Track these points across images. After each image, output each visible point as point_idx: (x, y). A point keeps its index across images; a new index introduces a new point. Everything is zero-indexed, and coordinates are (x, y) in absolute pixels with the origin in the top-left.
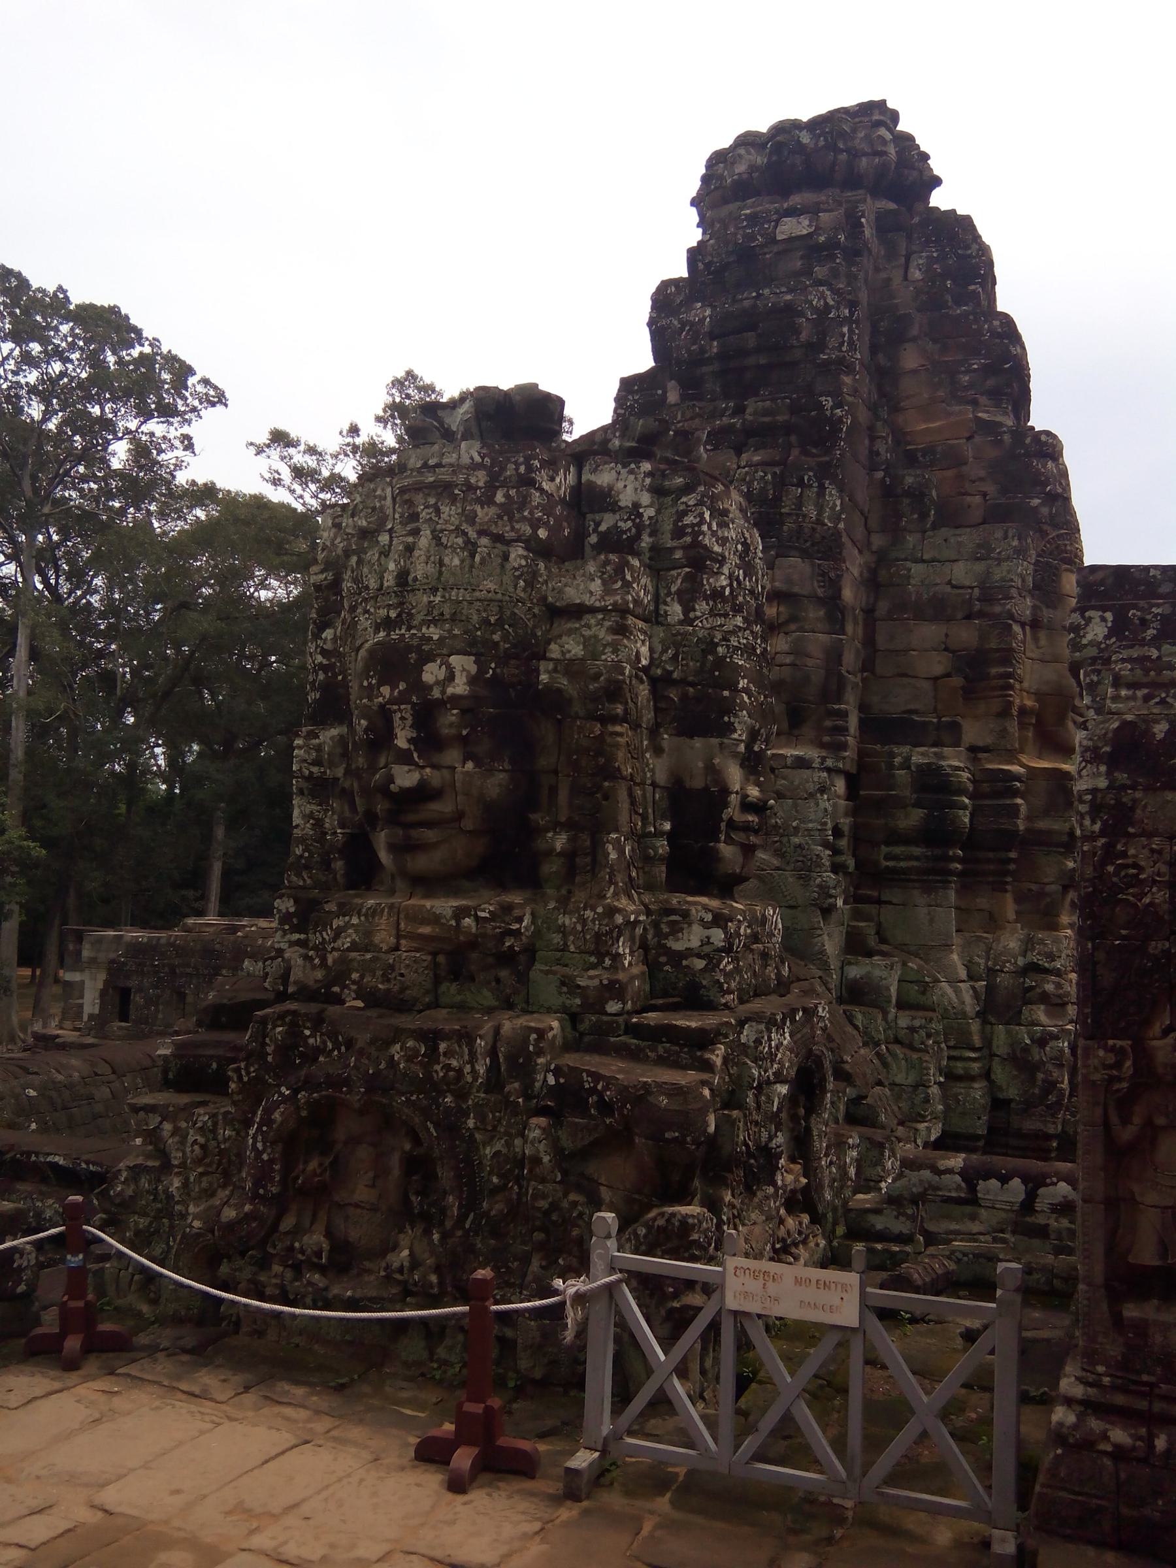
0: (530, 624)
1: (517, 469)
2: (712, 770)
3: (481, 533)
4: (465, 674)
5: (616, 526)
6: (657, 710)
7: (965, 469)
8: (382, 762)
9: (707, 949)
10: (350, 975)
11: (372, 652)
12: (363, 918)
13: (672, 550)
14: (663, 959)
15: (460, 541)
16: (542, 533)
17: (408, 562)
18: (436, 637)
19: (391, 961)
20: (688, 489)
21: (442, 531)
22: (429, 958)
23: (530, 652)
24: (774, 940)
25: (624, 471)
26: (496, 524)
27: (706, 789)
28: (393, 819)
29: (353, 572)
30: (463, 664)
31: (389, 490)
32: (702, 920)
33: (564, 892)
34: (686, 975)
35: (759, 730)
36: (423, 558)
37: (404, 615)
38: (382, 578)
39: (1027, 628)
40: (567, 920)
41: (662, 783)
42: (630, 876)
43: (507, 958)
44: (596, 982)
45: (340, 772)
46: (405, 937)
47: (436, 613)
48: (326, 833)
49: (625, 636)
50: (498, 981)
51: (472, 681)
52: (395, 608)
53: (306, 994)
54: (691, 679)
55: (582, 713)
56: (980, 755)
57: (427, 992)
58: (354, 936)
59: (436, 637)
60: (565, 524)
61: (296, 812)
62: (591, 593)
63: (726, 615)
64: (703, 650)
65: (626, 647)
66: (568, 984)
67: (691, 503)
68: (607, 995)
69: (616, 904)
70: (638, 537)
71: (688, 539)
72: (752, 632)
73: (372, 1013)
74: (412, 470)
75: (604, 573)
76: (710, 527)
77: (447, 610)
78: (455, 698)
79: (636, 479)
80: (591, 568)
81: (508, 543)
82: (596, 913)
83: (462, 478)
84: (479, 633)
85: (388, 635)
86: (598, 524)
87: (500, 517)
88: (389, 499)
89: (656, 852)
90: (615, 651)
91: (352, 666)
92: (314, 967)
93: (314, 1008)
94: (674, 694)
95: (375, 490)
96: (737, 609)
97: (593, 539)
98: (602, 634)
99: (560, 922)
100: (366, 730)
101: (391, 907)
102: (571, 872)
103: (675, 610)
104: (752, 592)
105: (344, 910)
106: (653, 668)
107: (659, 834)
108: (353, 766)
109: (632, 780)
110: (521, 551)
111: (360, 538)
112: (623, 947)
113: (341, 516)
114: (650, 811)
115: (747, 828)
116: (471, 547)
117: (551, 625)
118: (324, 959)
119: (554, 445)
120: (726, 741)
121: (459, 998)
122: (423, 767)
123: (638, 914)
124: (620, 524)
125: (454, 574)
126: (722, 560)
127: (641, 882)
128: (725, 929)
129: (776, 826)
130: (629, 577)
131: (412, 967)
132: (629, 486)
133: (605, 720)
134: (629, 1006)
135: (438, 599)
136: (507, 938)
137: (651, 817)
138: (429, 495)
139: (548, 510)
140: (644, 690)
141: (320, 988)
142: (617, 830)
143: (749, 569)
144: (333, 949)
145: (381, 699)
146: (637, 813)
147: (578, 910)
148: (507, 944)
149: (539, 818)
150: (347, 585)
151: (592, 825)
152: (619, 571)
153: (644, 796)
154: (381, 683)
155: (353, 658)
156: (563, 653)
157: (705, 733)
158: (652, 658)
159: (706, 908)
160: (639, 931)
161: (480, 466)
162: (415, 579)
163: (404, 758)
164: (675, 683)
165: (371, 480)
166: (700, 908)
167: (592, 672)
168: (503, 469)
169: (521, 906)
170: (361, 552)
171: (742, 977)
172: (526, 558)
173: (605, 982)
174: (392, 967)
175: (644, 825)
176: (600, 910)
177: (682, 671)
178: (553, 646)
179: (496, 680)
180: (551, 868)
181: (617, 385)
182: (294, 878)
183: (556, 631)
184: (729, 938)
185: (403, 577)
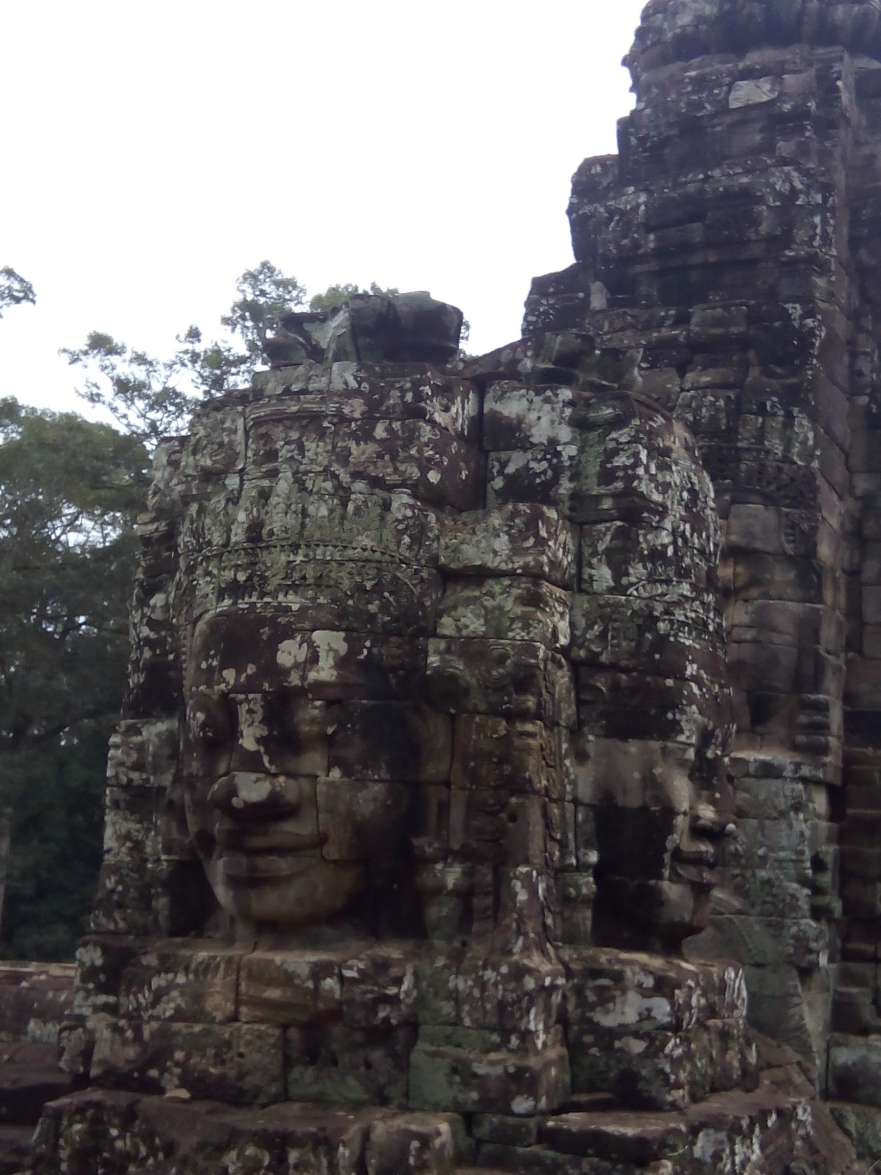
0: (417, 591)
1: (402, 397)
2: (651, 783)
3: (356, 475)
4: (331, 654)
5: (527, 468)
6: (579, 702)
8: (222, 767)
9: (647, 1026)
10: (172, 1053)
11: (213, 625)
12: (191, 976)
13: (599, 498)
14: (588, 1039)
15: (329, 485)
16: (433, 477)
17: (263, 512)
18: (295, 607)
19: (227, 1036)
20: (619, 422)
21: (306, 473)
22: (277, 1032)
23: (416, 626)
24: (736, 1013)
25: (537, 400)
26: (375, 464)
28: (235, 844)
29: (192, 523)
30: (330, 642)
31: (240, 422)
32: (640, 985)
33: (457, 944)
34: (619, 1061)
35: (713, 730)
36: (282, 506)
37: (256, 579)
38: (229, 531)
40: (461, 983)
41: (587, 800)
42: (544, 925)
43: (381, 1035)
44: (499, 1070)
45: (167, 779)
46: (246, 1003)
47: (296, 575)
48: (146, 860)
50: (368, 1065)
51: (341, 663)
52: (245, 570)
53: (115, 1079)
54: (624, 663)
55: (482, 707)
57: (274, 1079)
58: (179, 1001)
59: (295, 607)
60: (462, 464)
61: (109, 832)
62: (495, 553)
63: (668, 582)
64: (639, 626)
65: (540, 621)
66: (460, 1070)
67: (623, 440)
68: (513, 1088)
69: (526, 961)
70: (555, 481)
71: (620, 485)
72: (703, 603)
73: (201, 1107)
74: (270, 397)
75: (511, 527)
76: (647, 470)
77: (311, 572)
78: (319, 686)
79: (553, 409)
80: (496, 520)
81: (391, 488)
82: (499, 973)
83: (332, 407)
84: (350, 602)
85: (235, 603)
86: (504, 465)
87: (380, 456)
88: (241, 432)
89: (578, 890)
90: (526, 627)
91: (187, 642)
92: (125, 1042)
93: (123, 1098)
94: (601, 683)
95: (223, 422)
96: (683, 574)
97: (498, 483)
98: (509, 605)
99: (451, 985)
100: (203, 726)
101: (229, 961)
102: (466, 917)
103: (603, 575)
104: (702, 552)
105: (167, 965)
106: (575, 649)
107: (582, 867)
108: (185, 773)
109: (547, 795)
110: (406, 499)
111: (201, 481)
112: (535, 1022)
113: (180, 452)
114: (571, 836)
115: (698, 861)
116: (343, 493)
117: (444, 591)
118: (138, 1031)
119: (449, 366)
120: (670, 744)
121: (315, 1089)
122: (275, 775)
123: (554, 975)
124: (533, 465)
125: (320, 527)
126: (662, 511)
127: (559, 932)
128: (671, 998)
129: (736, 855)
130: (543, 533)
131: (255, 1046)
132: (545, 418)
134: (543, 1103)
135: (299, 558)
136: (381, 1006)
137: (572, 846)
138: (291, 428)
139: (440, 446)
140: (562, 678)
141: (132, 1071)
142: (527, 862)
143: (697, 521)
144: (151, 1018)
145: (223, 686)
146: (553, 839)
147: (475, 969)
148: (381, 1015)
149: (425, 844)
150: (184, 539)
151: (495, 854)
152: (531, 525)
153: (563, 816)
154: (223, 666)
155: (189, 633)
156: (459, 630)
158: (573, 636)
159: (646, 970)
160: (556, 999)
161: (357, 393)
162: (271, 533)
163: (252, 763)
164: (603, 668)
165: (217, 409)
166: (637, 969)
167: (496, 653)
168: (385, 397)
169: (401, 963)
170: (203, 498)
171: (694, 1065)
172: (412, 507)
173: (511, 1070)
174: (228, 1044)
175: (563, 856)
176: (504, 970)
177: (612, 653)
178: (446, 620)
180: (439, 911)
181: (528, 287)
182: (103, 920)
183: (449, 601)
184: (677, 1011)
185: (255, 530)
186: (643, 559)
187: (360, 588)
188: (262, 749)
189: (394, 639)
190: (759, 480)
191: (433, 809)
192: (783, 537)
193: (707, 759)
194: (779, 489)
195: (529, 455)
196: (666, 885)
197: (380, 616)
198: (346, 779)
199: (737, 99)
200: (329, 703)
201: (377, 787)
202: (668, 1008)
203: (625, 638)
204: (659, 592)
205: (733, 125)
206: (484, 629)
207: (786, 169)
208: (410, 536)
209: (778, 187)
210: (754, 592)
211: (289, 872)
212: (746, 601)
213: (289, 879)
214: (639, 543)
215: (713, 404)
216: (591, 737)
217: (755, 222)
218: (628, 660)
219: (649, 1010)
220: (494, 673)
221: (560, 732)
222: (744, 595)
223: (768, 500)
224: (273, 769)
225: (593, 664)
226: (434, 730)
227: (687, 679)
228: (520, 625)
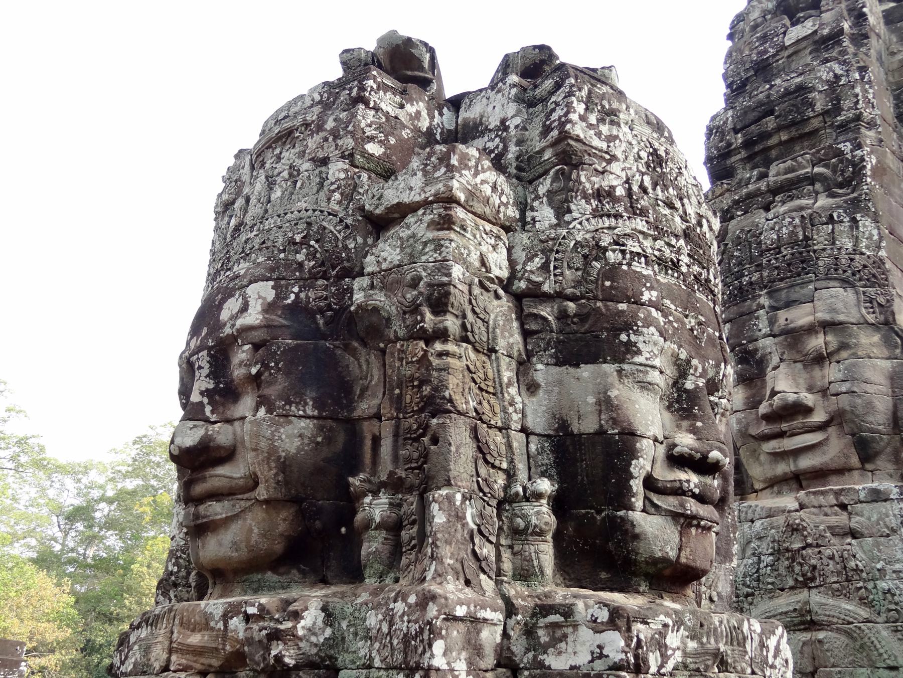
2: (605, 403)
6: (526, 334)
27: (601, 432)
41: (539, 430)
49: (450, 229)
54: (569, 291)
55: (401, 333)
62: (411, 189)
64: (585, 257)
65: (452, 241)
94: (546, 311)
103: (545, 215)
133: (430, 338)
151: (420, 479)
153: (509, 446)
157: (593, 359)
164: (546, 298)
178: (370, 259)
179: (297, 309)
186: (586, 197)
187: (292, 242)
188: (206, 400)
189: (321, 282)
190: (836, 270)
191: (368, 443)
192: (864, 311)
193: (687, 391)
194: (854, 274)
195: (486, 139)
196: (637, 516)
197: (306, 262)
198: (268, 415)
199: (790, 39)
200: (256, 347)
201: (303, 423)
202: (622, 643)
203: (569, 267)
204: (607, 225)
205: (789, 57)
206: (399, 257)
207: (828, 65)
208: (342, 194)
209: (824, 78)
210: (844, 354)
211: (224, 516)
212: (838, 362)
213: (227, 521)
214: (580, 183)
215: (790, 223)
216: (540, 366)
217: (812, 105)
218: (574, 287)
219: (600, 647)
220: (408, 296)
221: (497, 358)
222: (836, 357)
223: (846, 283)
224: (213, 418)
225: (535, 294)
226: (365, 367)
227: (643, 304)
228: (433, 246)
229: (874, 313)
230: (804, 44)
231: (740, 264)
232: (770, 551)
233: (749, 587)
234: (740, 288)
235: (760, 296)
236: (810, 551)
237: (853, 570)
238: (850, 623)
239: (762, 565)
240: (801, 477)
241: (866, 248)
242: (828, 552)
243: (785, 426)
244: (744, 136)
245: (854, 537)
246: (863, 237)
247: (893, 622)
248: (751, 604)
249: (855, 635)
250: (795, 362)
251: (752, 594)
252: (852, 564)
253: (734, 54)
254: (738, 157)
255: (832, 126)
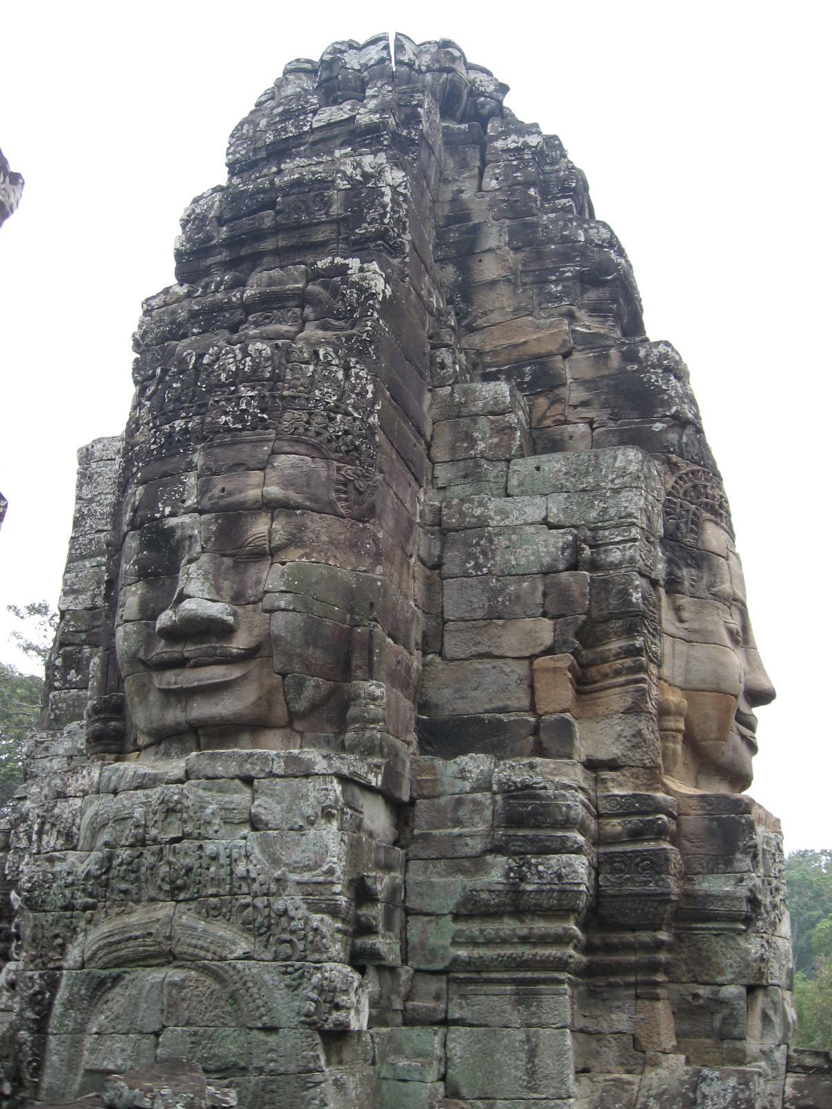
7: (563, 392)
39: (662, 590)
56: (607, 775)
212: (283, 564)
217: (327, 204)
229: (346, 500)
230: (336, 131)
231: (178, 399)
232: (131, 840)
233: (90, 895)
234: (169, 436)
235: (195, 451)
236: (186, 843)
237: (243, 878)
238: (223, 959)
239: (115, 863)
240: (200, 732)
241: (354, 407)
242: (210, 848)
243: (189, 650)
244: (231, 230)
245: (255, 829)
246: (352, 392)
247: (284, 960)
248: (89, 922)
249: (226, 976)
250: (223, 555)
251: (93, 907)
252: (241, 869)
253: (246, 127)
254: (218, 258)
255: (346, 240)
